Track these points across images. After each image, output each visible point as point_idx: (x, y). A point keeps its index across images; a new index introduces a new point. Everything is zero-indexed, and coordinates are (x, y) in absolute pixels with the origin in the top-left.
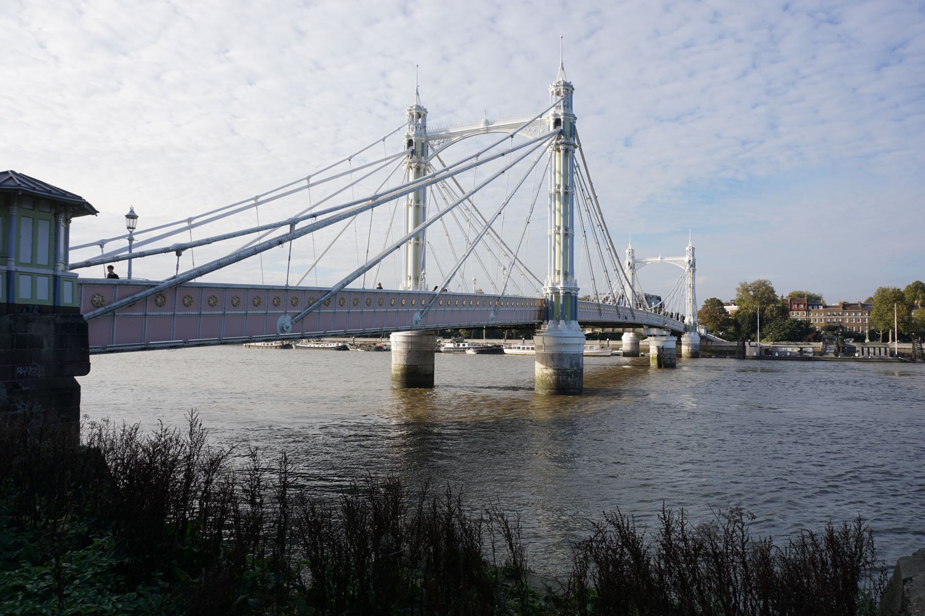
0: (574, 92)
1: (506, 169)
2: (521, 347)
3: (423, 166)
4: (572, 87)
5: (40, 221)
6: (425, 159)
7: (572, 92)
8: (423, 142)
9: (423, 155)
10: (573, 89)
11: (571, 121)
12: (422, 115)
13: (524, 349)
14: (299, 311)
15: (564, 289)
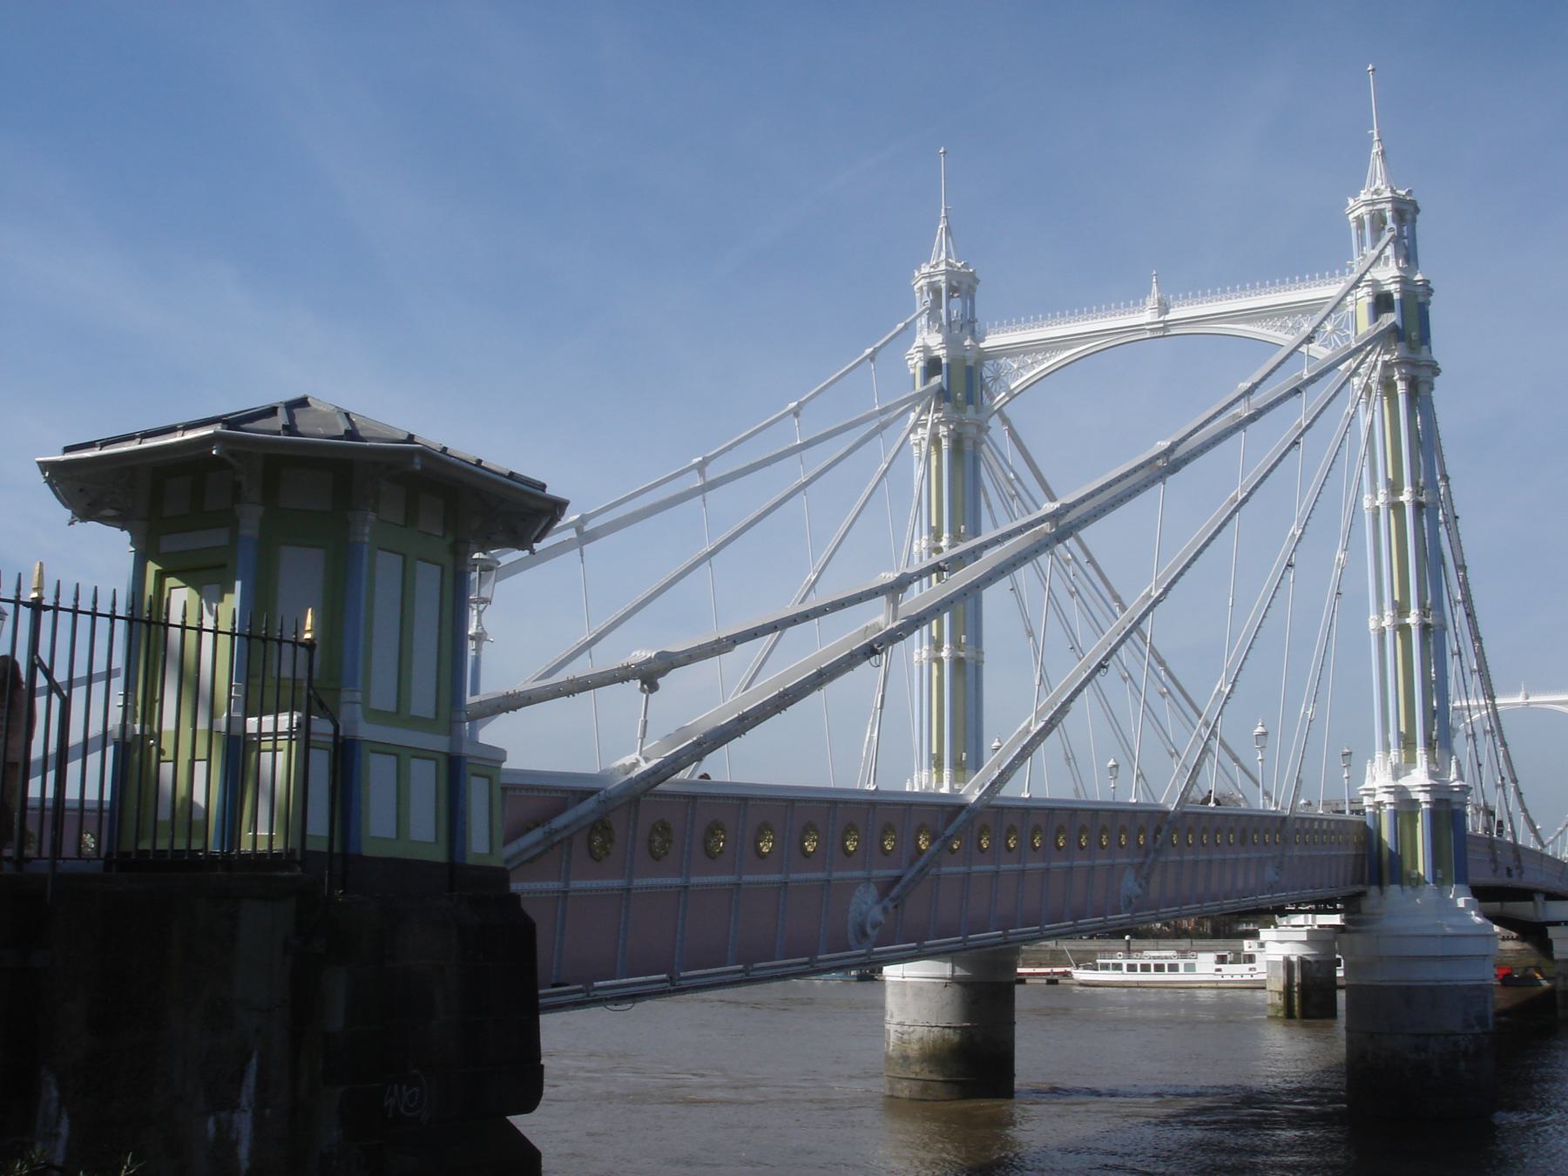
0: (1419, 217)
1: (1301, 435)
2: (1125, 963)
3: (971, 431)
4: (1413, 203)
5: (379, 552)
6: (977, 412)
7: (1414, 221)
8: (970, 363)
9: (970, 399)
10: (1417, 210)
11: (1421, 299)
12: (964, 287)
13: (1132, 968)
14: (895, 872)
15: (1433, 790)
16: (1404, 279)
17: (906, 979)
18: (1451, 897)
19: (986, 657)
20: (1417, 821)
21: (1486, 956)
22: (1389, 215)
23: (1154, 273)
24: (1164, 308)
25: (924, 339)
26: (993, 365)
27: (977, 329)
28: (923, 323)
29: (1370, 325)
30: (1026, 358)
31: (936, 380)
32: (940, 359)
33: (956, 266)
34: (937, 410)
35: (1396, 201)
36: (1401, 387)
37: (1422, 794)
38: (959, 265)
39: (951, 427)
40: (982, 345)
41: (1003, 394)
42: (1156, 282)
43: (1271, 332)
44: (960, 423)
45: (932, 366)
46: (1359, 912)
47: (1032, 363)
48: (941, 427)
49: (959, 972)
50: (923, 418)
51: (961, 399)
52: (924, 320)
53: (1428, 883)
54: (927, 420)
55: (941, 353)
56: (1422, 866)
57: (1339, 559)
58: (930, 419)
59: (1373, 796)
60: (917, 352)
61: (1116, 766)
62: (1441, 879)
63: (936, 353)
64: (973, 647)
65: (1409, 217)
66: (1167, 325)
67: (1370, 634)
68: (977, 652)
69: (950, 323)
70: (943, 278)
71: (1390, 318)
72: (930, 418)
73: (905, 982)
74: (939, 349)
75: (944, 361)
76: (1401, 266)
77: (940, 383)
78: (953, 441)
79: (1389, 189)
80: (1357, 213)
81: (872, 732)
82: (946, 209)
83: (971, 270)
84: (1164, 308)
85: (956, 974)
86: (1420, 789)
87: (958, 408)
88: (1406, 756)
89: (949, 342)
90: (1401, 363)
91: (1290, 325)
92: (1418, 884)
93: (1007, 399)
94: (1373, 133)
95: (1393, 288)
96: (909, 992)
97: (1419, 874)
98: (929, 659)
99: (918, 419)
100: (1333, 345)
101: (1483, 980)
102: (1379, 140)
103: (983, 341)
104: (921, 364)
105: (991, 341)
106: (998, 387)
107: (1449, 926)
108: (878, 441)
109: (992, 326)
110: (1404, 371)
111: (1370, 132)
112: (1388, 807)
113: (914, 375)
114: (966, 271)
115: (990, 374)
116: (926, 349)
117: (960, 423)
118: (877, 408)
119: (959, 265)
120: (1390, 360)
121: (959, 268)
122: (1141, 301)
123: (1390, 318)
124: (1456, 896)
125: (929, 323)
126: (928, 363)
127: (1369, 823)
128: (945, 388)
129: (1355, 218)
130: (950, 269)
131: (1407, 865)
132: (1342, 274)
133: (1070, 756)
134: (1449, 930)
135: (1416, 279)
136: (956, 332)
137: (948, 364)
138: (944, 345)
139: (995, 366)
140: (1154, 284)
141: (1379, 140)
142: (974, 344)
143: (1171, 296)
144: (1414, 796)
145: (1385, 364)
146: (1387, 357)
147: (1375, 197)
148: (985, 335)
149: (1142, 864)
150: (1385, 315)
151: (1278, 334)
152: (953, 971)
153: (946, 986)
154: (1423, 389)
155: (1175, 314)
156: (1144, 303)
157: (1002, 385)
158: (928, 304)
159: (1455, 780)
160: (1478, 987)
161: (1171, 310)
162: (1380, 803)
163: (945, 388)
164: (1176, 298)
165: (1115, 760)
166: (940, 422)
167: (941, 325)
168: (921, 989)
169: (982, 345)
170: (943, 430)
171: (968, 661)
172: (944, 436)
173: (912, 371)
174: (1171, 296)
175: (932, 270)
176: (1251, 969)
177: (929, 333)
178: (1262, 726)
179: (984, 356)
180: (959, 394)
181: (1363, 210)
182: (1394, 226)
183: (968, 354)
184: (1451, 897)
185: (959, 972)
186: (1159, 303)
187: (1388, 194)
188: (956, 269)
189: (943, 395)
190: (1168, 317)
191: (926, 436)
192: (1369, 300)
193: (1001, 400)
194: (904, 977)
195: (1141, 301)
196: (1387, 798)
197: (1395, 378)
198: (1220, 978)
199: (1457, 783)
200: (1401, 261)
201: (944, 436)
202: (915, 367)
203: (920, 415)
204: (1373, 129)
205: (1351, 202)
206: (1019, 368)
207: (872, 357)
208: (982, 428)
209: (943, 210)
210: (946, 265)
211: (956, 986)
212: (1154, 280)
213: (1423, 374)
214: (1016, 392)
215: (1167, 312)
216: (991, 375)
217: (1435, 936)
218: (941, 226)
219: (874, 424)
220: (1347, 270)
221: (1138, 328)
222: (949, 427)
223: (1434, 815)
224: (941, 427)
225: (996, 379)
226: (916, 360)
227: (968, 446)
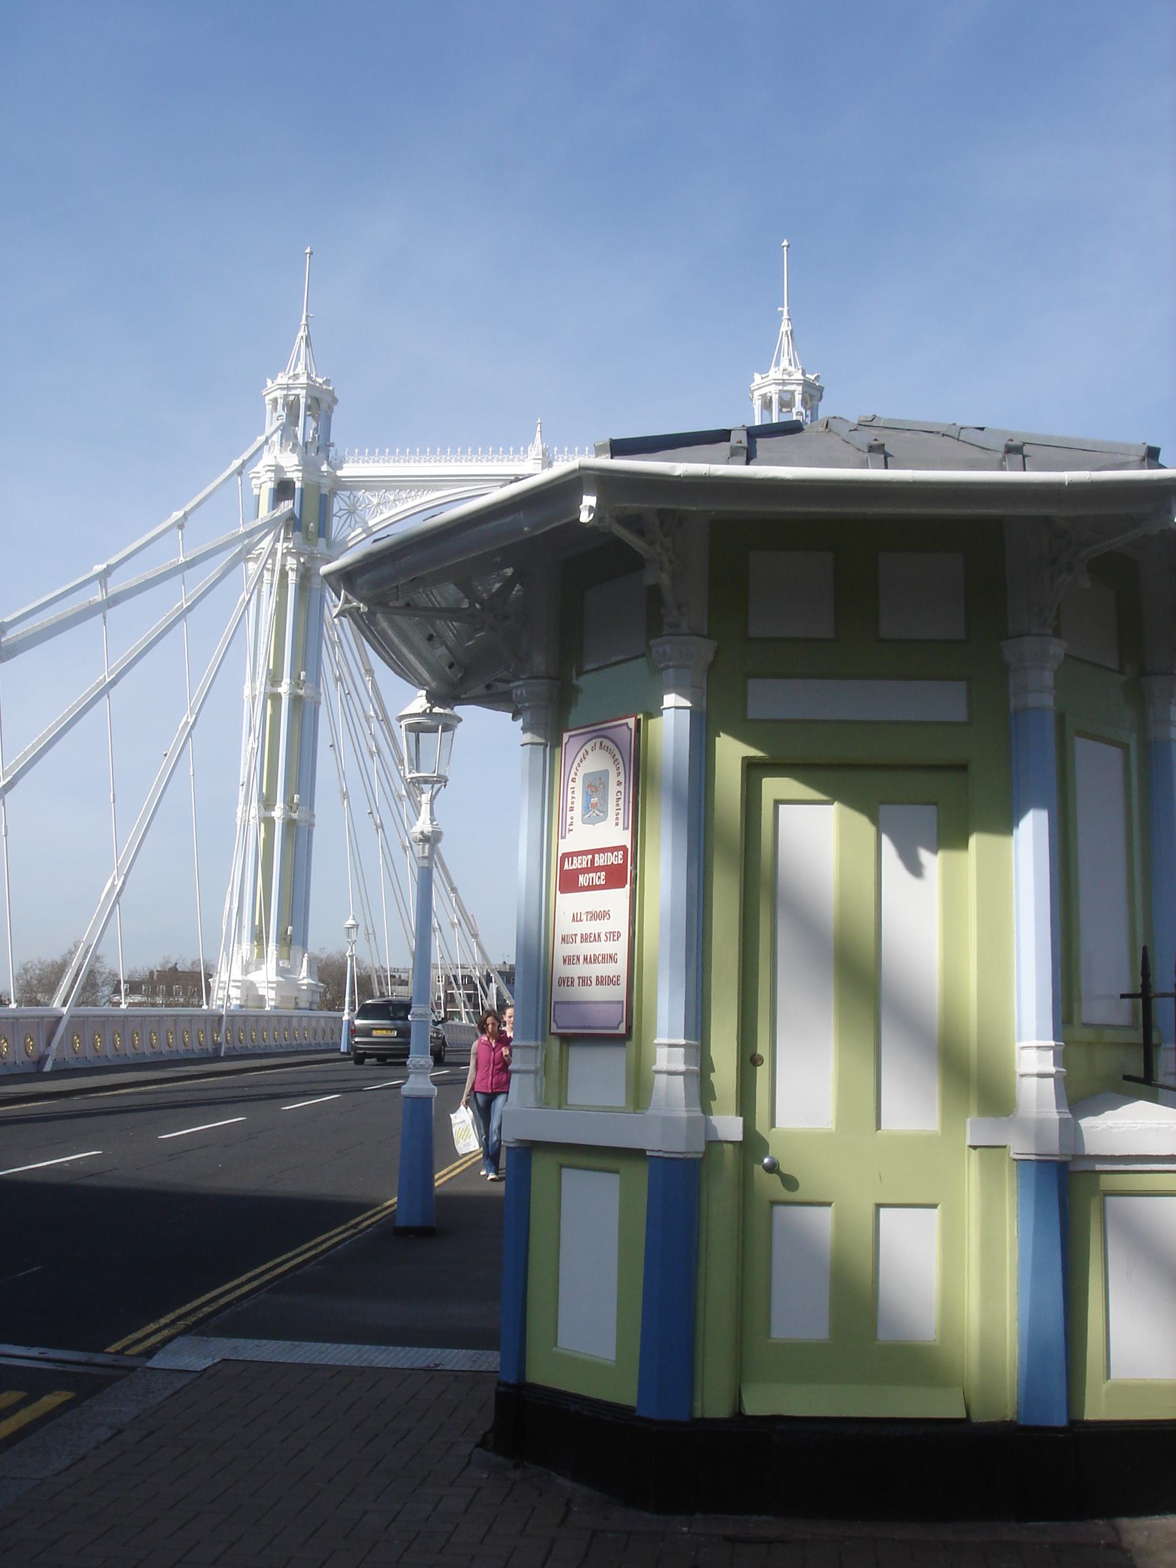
8: (325, 491)
19: (317, 821)
23: (539, 421)
25: (276, 457)
26: (349, 498)
30: (387, 494)
31: (286, 506)
33: (317, 382)
34: (286, 539)
39: (302, 560)
41: (359, 530)
44: (312, 558)
45: (283, 489)
47: (394, 500)
48: (289, 558)
51: (313, 530)
52: (276, 438)
63: (289, 475)
69: (306, 444)
72: (281, 547)
74: (294, 471)
75: (298, 485)
77: (292, 510)
78: (301, 575)
82: (307, 316)
83: (331, 388)
89: (307, 465)
93: (364, 536)
94: (782, 311)
102: (789, 319)
103: (341, 468)
104: (271, 485)
105: (348, 470)
106: (353, 522)
109: (352, 453)
111: (780, 309)
114: (327, 387)
115: (344, 506)
116: (278, 469)
117: (312, 558)
119: (320, 381)
121: (320, 384)
122: (522, 449)
125: (281, 440)
126: (278, 485)
128: (298, 516)
133: (371, 931)
136: (313, 455)
138: (301, 468)
139: (352, 497)
140: (538, 435)
141: (789, 319)
142: (331, 470)
143: (556, 449)
156: (526, 452)
157: (358, 519)
158: (283, 420)
163: (298, 516)
164: (561, 452)
167: (295, 445)
169: (339, 473)
170: (291, 562)
172: (292, 570)
173: (256, 492)
174: (556, 449)
179: (340, 485)
180: (312, 524)
183: (323, 481)
186: (544, 454)
187: (798, 376)
188: (318, 385)
189: (293, 523)
193: (354, 538)
195: (522, 449)
201: (292, 570)
204: (783, 307)
206: (378, 504)
210: (307, 378)
212: (539, 429)
214: (374, 530)
216: (347, 508)
218: (300, 335)
222: (299, 561)
224: (289, 558)
225: (351, 512)
226: (262, 480)
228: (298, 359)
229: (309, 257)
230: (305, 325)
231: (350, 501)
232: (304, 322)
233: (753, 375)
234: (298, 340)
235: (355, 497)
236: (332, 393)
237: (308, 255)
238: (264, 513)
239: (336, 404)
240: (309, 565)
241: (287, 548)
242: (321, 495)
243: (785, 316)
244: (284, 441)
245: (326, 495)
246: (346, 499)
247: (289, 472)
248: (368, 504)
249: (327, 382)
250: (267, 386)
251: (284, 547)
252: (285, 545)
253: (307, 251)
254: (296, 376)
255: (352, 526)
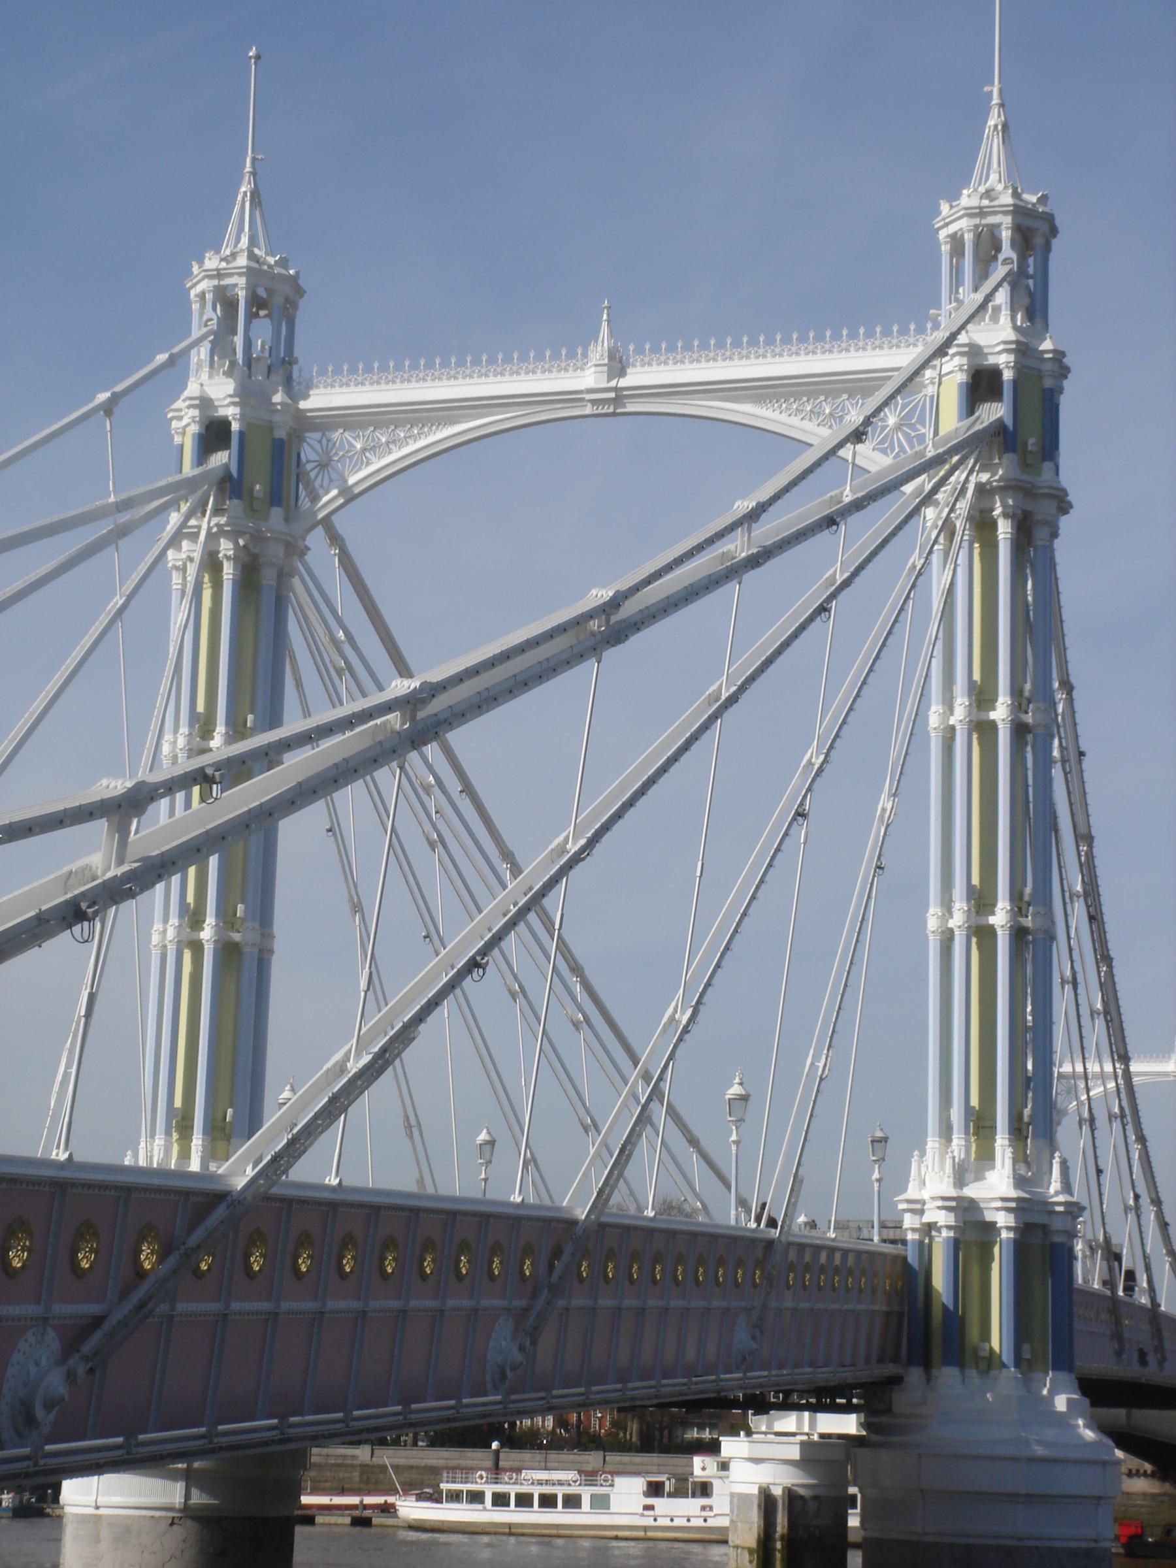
0: (1055, 243)
1: (833, 596)
2: (489, 1490)
3: (276, 551)
4: (1049, 219)
6: (287, 519)
7: (1047, 248)
8: (280, 434)
9: (276, 496)
10: (1054, 231)
11: (1048, 383)
12: (278, 301)
13: (500, 1500)
14: (92, 1309)
15: (1021, 1208)
16: (1023, 348)
17: (101, 1511)
18: (1045, 1392)
20: (993, 1259)
21: (1100, 1498)
22: (1006, 235)
24: (617, 365)
25: (202, 385)
26: (320, 442)
27: (295, 375)
28: (202, 356)
29: (960, 419)
31: (220, 459)
32: (230, 424)
33: (265, 263)
34: (217, 511)
35: (1020, 212)
36: (1004, 529)
37: (1003, 1213)
38: (271, 260)
39: (241, 542)
40: (303, 405)
41: (334, 492)
42: (609, 321)
43: (795, 421)
44: (257, 537)
46: (889, 1410)
48: (222, 540)
49: (198, 1498)
50: (193, 522)
51: (261, 496)
52: (204, 351)
53: (1004, 1366)
54: (199, 527)
55: (231, 413)
56: (998, 1338)
57: (884, 810)
58: (205, 526)
59: (921, 1212)
60: (189, 407)
61: (491, 1143)
62: (1030, 1362)
64: (257, 925)
65: (1038, 241)
66: (620, 397)
67: (927, 940)
68: (263, 935)
69: (249, 362)
70: (242, 281)
71: (994, 412)
72: (205, 523)
73: (100, 1517)
75: (235, 426)
76: (1019, 323)
77: (226, 467)
79: (1010, 191)
80: (952, 229)
81: (69, 1065)
82: (254, 160)
83: (292, 272)
84: (617, 365)
85: (192, 1502)
86: (999, 1204)
87: (255, 511)
88: (977, 1147)
89: (246, 395)
90: (1009, 487)
91: (827, 411)
92: (989, 1367)
93: (341, 501)
94: (991, 92)
95: (1004, 361)
96: (105, 1533)
97: (991, 1349)
98: (179, 942)
99: (184, 524)
100: (897, 450)
101: (1095, 1541)
103: (306, 396)
104: (194, 429)
105: (318, 400)
107: (1041, 1443)
108: (112, 557)
109: (323, 372)
110: (1010, 502)
111: (986, 89)
112: (945, 1233)
113: (182, 446)
114: (283, 271)
115: (312, 456)
116: (205, 403)
118: (112, 499)
119: (271, 260)
120: (989, 482)
121: (270, 267)
122: (580, 351)
123: (994, 412)
124: (1053, 1392)
127: (913, 1259)
128: (235, 474)
129: (948, 236)
130: (256, 265)
131: (973, 1333)
132: (921, 330)
134: (1039, 1451)
135: (1042, 348)
137: (242, 434)
138: (237, 400)
139: (324, 441)
140: (605, 325)
142: (289, 401)
143: (631, 347)
144: (989, 1216)
145: (981, 489)
146: (984, 477)
147: (986, 202)
148: (309, 386)
149: (526, 1310)
150: (987, 405)
151: (808, 425)
152: (187, 1496)
153: (172, 1524)
154: (1041, 534)
155: (636, 377)
156: (585, 355)
157: (334, 475)
158: (213, 325)
159: (1057, 1193)
160: (1088, 1552)
161: (629, 371)
162: (930, 1227)
163: (235, 474)
164: (640, 351)
165: (489, 1133)
166: (221, 532)
167: (233, 364)
168: (128, 1529)
169: (303, 405)
170: (226, 547)
171: (247, 950)
172: (228, 558)
173: (177, 440)
174: (631, 347)
175: (224, 264)
176: (703, 1508)
177: (211, 376)
178: (741, 1084)
179: (304, 424)
180: (258, 487)
181: (964, 224)
182: (1014, 256)
183: (277, 418)
184: (1045, 1392)
185: (198, 1498)
187: (1007, 199)
188: (265, 267)
190: (623, 382)
191: (197, 556)
192: (962, 377)
194: (97, 1508)
195: (580, 351)
196: (943, 1218)
197: (996, 513)
198: (649, 1522)
199: (1061, 1198)
200: (1019, 316)
201: (228, 558)
202: (184, 433)
203: (188, 517)
204: (992, 84)
205: (945, 208)
206: (364, 450)
207: (108, 409)
208: (296, 549)
209: (248, 160)
211: (189, 1523)
212: (605, 317)
213: (1044, 509)
214: (357, 490)
215: (622, 373)
216: (317, 458)
217: (1015, 1459)
218: (243, 189)
219: (103, 528)
220: (929, 325)
221: (571, 398)
222: (236, 544)
223: (1022, 1250)
224: (222, 540)
225: (323, 465)
226: (185, 421)
227: (268, 577)
228: (241, 229)
229: (255, 63)
230: (250, 173)
231: (322, 446)
232: (248, 168)
233: (939, 205)
234: (240, 198)
235: (328, 441)
236: (294, 281)
237: (253, 61)
238: (188, 469)
239: (302, 296)
240: (256, 550)
241: (217, 525)
242: (274, 440)
243: (996, 100)
244: (216, 358)
245: (281, 440)
246: (317, 446)
247: (220, 406)
248: (348, 451)
249: (283, 263)
250: (193, 273)
251: (212, 524)
252: (215, 520)
253: (251, 54)
254: (234, 255)
255: (325, 485)
